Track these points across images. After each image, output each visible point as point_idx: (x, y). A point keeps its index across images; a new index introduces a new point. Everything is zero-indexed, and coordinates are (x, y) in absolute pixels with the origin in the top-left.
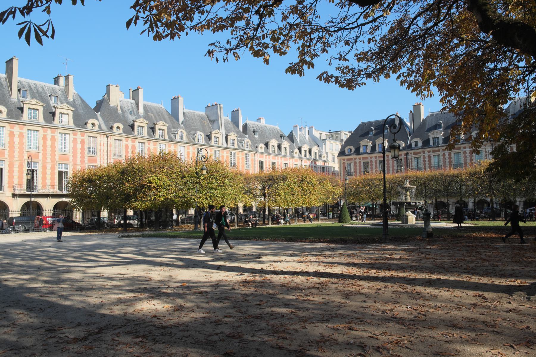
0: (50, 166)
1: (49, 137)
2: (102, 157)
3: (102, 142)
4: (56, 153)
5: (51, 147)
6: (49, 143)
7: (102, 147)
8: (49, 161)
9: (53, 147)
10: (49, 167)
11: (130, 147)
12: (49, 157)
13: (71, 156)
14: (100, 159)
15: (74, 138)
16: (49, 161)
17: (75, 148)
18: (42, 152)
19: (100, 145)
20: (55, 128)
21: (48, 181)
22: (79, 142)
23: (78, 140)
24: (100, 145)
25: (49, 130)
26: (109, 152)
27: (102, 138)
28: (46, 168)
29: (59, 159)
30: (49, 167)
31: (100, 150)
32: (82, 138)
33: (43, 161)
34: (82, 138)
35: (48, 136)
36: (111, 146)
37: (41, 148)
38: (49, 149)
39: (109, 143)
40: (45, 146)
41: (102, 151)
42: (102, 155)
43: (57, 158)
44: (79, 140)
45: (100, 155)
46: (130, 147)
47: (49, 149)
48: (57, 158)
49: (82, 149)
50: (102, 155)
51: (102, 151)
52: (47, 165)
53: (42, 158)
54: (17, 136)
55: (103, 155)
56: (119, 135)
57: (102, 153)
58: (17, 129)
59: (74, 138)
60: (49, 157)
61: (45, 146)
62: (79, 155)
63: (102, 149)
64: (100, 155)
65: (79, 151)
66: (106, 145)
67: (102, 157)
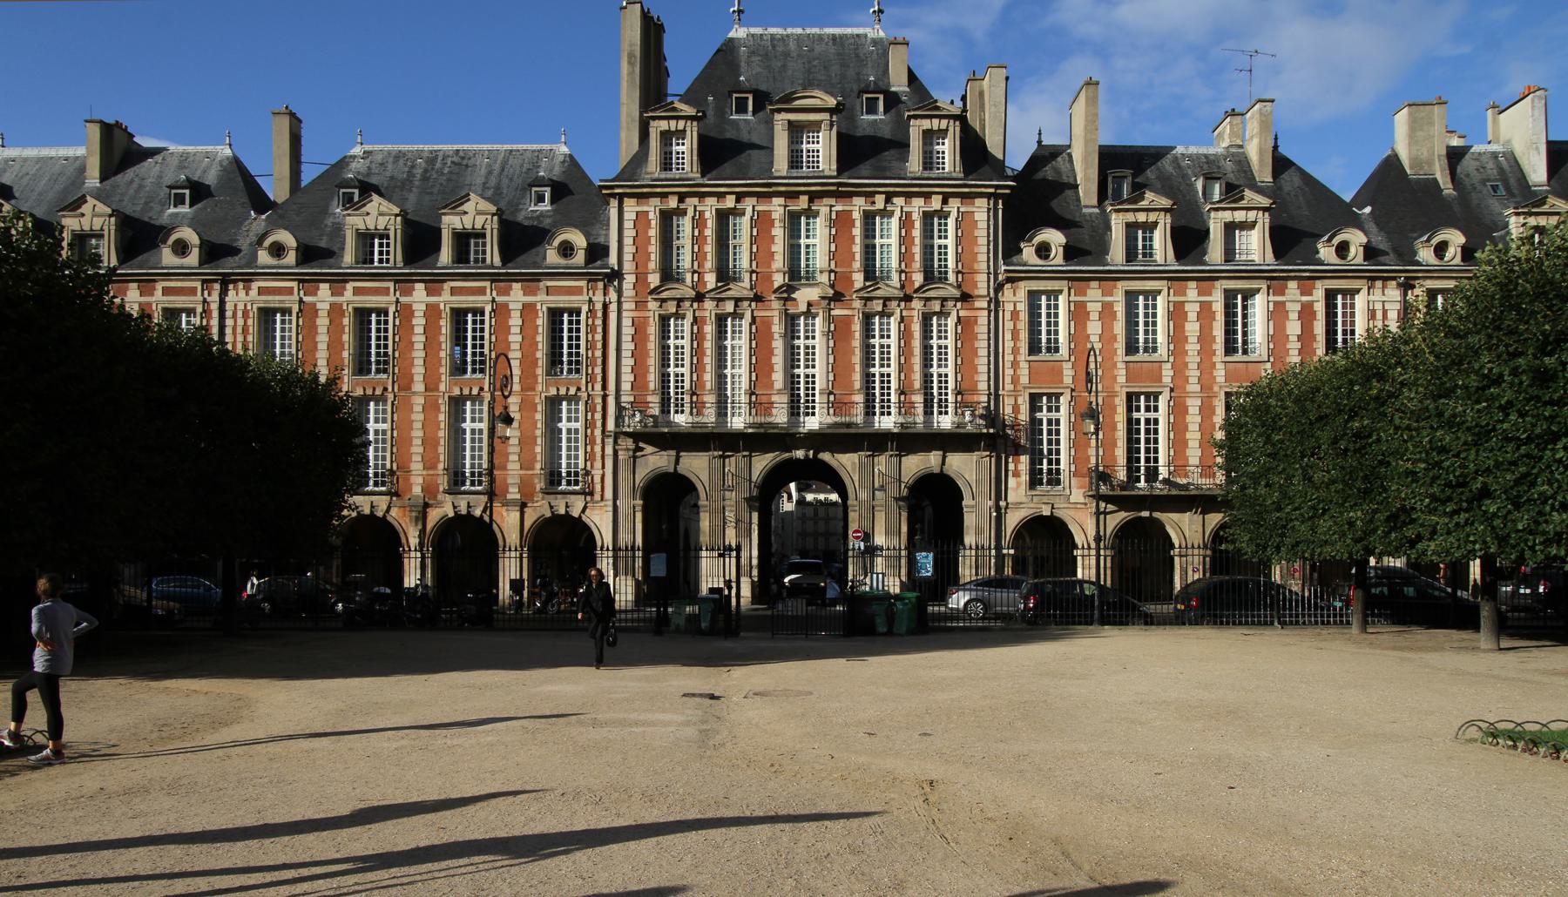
1: (1192, 310)
3: (1378, 306)
4: (1215, 359)
8: (1193, 387)
10: (1193, 405)
12: (1193, 373)
16: (1193, 387)
20: (1210, 278)
21: (1194, 455)
22: (1294, 316)
23: (1289, 306)
25: (1192, 284)
27: (1378, 291)
28: (1186, 411)
30: (1193, 405)
32: (1305, 298)
34: (1305, 298)
35: (1188, 307)
38: (1192, 347)
40: (1178, 338)
44: (1293, 309)
47: (1192, 347)
52: (1189, 402)
54: (1094, 316)
58: (1094, 293)
60: (1193, 373)
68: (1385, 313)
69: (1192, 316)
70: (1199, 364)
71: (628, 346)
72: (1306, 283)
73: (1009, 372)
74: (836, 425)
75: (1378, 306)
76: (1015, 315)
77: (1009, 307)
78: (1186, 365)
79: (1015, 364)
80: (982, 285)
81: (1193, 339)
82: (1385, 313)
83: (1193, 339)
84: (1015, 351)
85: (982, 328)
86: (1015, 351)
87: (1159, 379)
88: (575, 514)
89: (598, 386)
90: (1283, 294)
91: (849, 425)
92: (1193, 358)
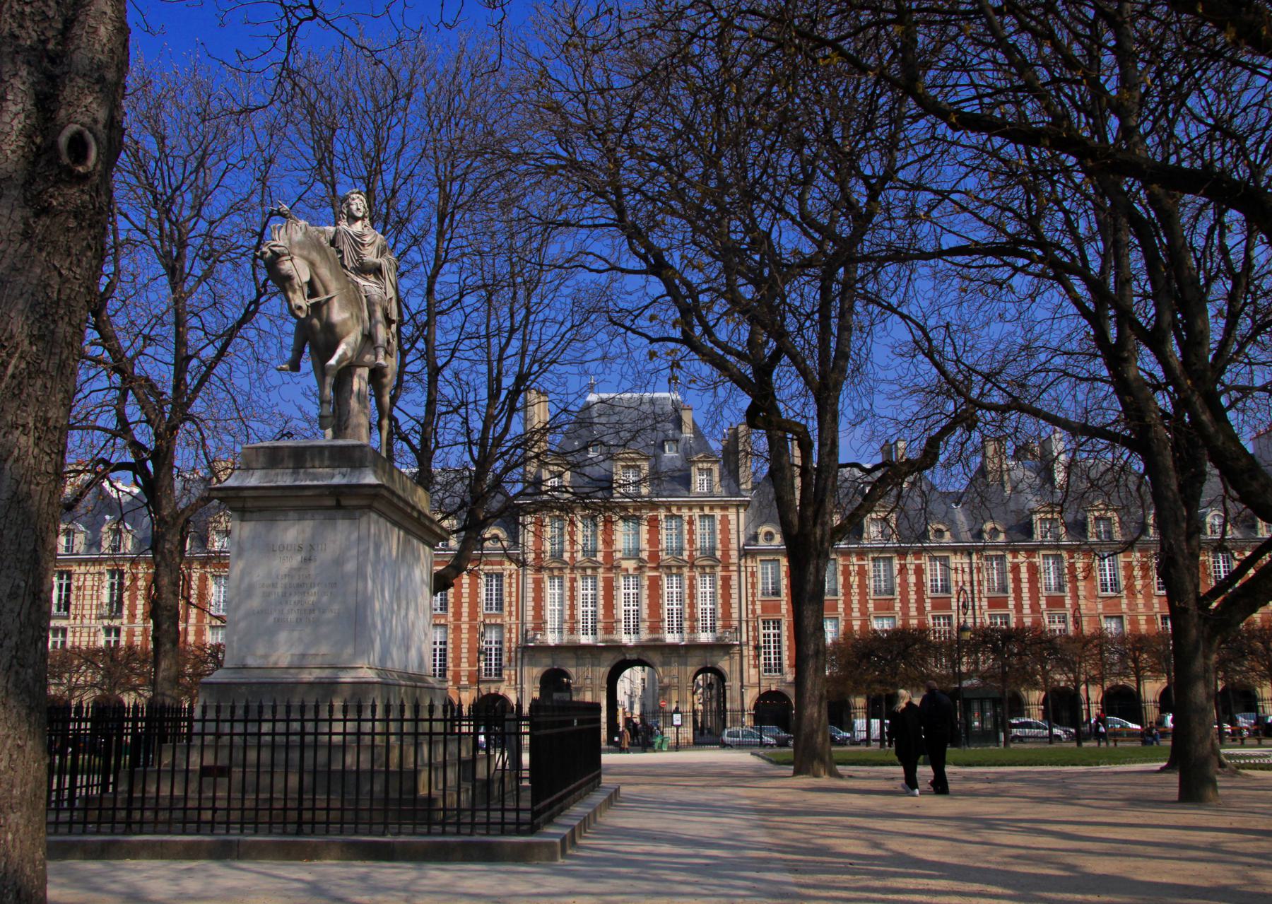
5: (859, 586)
6: (854, 580)
8: (856, 614)
11: (1024, 569)
12: (855, 606)
16: (856, 614)
37: (841, 591)
40: (848, 586)
43: (871, 606)
46: (1024, 569)
47: (855, 590)
48: (871, 606)
49: (920, 585)
56: (996, 548)
60: (855, 606)
61: (848, 586)
62: (913, 596)
63: (960, 579)
65: (912, 589)
71: (530, 595)
73: (750, 607)
74: (650, 640)
76: (753, 574)
77: (749, 569)
79: (753, 603)
80: (734, 555)
84: (754, 595)
85: (734, 582)
86: (754, 595)
87: (836, 609)
88: (500, 693)
89: (513, 618)
91: (657, 640)
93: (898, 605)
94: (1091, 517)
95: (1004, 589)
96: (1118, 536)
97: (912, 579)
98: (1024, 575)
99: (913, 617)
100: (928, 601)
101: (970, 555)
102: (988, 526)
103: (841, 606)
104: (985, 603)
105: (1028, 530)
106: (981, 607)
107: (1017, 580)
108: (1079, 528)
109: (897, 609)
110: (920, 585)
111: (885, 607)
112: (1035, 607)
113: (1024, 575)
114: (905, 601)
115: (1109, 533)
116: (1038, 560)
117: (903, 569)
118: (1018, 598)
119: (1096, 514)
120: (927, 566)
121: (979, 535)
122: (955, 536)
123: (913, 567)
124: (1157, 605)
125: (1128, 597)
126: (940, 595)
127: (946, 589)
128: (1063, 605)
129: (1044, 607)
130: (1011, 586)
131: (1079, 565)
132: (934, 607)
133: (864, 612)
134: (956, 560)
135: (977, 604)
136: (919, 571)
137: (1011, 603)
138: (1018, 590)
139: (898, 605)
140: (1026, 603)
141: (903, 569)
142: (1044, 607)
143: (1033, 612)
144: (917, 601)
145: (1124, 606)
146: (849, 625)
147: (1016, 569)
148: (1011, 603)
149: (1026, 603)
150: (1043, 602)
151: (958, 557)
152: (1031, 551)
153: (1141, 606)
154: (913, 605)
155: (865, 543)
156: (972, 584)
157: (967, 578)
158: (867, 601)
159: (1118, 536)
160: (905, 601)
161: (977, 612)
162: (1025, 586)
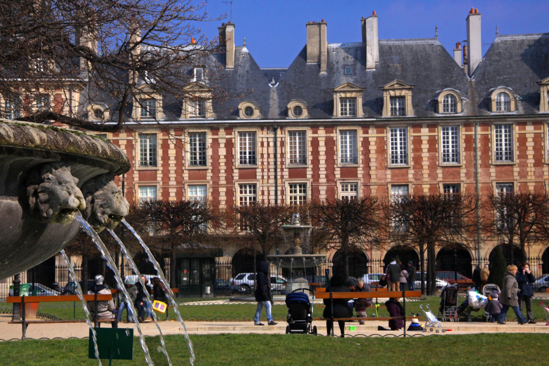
0: (175, 190)
2: (265, 167)
3: (265, 140)
5: (176, 158)
6: (172, 152)
7: (265, 149)
8: (173, 182)
9: (179, 158)
11: (322, 143)
12: (172, 175)
13: (210, 171)
14: (263, 170)
15: (213, 139)
16: (173, 182)
17: (215, 157)
18: (161, 168)
19: (262, 145)
22: (222, 145)
23: (220, 141)
24: (262, 145)
26: (279, 156)
29: (190, 178)
31: (262, 155)
33: (164, 183)
36: (283, 144)
38: (172, 162)
39: (279, 140)
41: (265, 156)
42: (265, 163)
43: (186, 175)
44: (222, 142)
45: (262, 163)
46: (322, 143)
47: (172, 162)
48: (186, 175)
49: (230, 156)
50: (265, 163)
51: (265, 156)
52: (170, 190)
53: (163, 178)
55: (268, 163)
57: (265, 160)
59: (213, 139)
60: (172, 175)
62: (223, 167)
63: (265, 151)
64: (262, 163)
65: (222, 161)
66: (272, 144)
67: (265, 167)
68: (268, 143)
69: (172, 146)
70: (176, 171)
72: (229, 129)
75: (265, 140)
78: (169, 171)
81: (172, 158)
82: (268, 143)
83: (172, 158)
87: (155, 178)
90: (217, 135)
92: (172, 168)
93: (209, 174)
94: (386, 97)
95: (304, 160)
96: (410, 112)
97: (222, 152)
98: (322, 149)
99: (222, 186)
100: (236, 171)
101: (275, 130)
102: (292, 105)
103: (160, 176)
104: (286, 173)
105: (329, 108)
106: (282, 177)
107: (315, 153)
108: (375, 106)
109: (209, 178)
110: (230, 156)
111: (197, 178)
112: (330, 177)
113: (322, 149)
114: (216, 171)
115: (403, 110)
116: (337, 136)
117: (215, 142)
118: (316, 169)
119: (392, 93)
120: (237, 141)
121: (284, 113)
122: (265, 114)
123: (224, 141)
124: (440, 175)
125: (414, 168)
126: (248, 166)
127: (253, 160)
128: (355, 175)
129: (338, 176)
130: (310, 158)
131: (373, 141)
132: (241, 177)
133: (180, 181)
134: (262, 135)
135: (279, 173)
136: (229, 145)
137: (309, 173)
138: (315, 162)
139: (209, 174)
140: (323, 173)
141: (215, 142)
142: (338, 176)
143: (328, 181)
144: (226, 171)
145: (410, 176)
146: (166, 193)
147: (315, 143)
148: (309, 173)
149: (323, 173)
150: (338, 173)
151: (265, 132)
152: (330, 127)
153: (426, 176)
154: (223, 175)
155: (182, 120)
156: (275, 157)
157: (271, 150)
158: (183, 172)
159: (410, 112)
160: (216, 171)
161: (279, 181)
162: (322, 158)
